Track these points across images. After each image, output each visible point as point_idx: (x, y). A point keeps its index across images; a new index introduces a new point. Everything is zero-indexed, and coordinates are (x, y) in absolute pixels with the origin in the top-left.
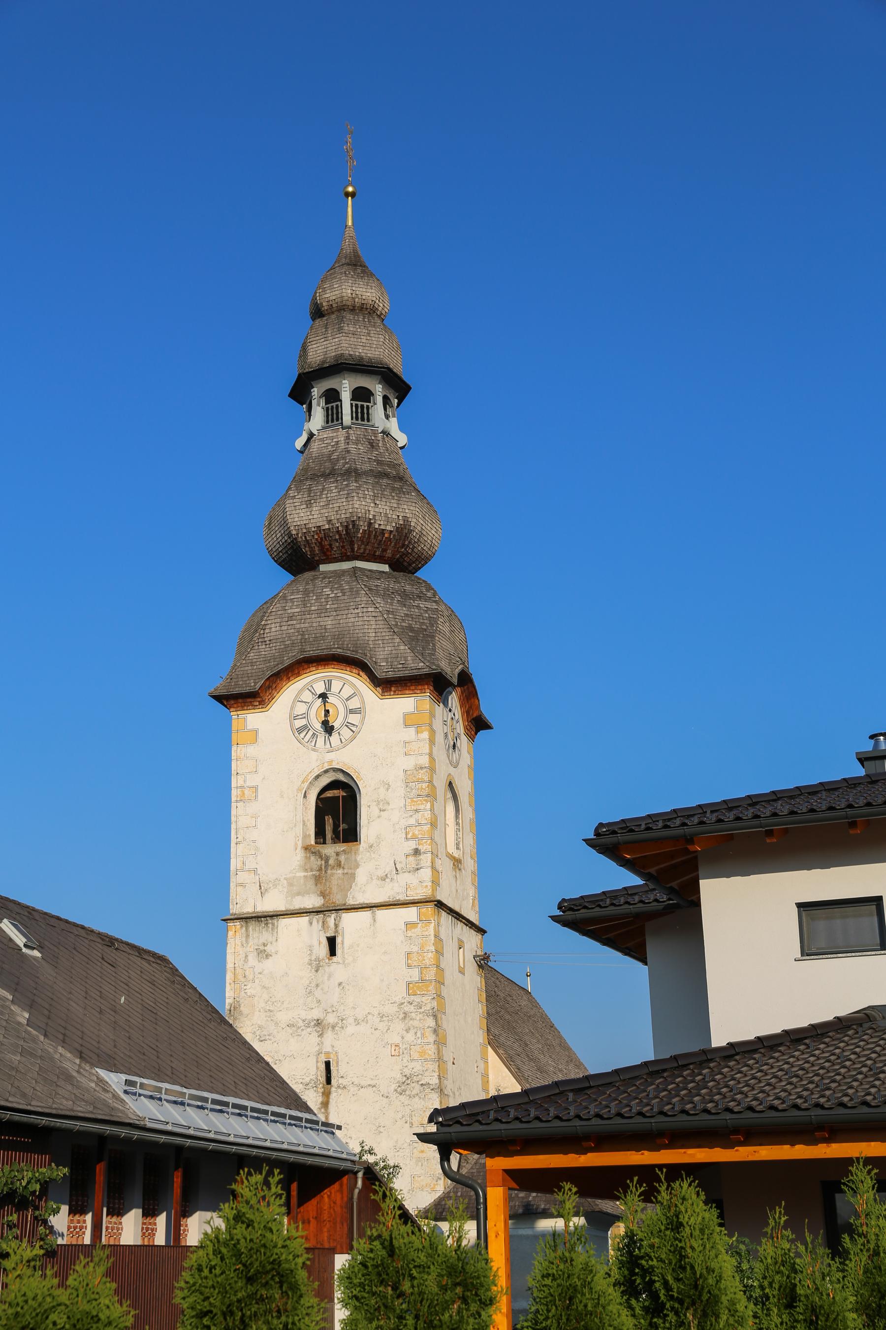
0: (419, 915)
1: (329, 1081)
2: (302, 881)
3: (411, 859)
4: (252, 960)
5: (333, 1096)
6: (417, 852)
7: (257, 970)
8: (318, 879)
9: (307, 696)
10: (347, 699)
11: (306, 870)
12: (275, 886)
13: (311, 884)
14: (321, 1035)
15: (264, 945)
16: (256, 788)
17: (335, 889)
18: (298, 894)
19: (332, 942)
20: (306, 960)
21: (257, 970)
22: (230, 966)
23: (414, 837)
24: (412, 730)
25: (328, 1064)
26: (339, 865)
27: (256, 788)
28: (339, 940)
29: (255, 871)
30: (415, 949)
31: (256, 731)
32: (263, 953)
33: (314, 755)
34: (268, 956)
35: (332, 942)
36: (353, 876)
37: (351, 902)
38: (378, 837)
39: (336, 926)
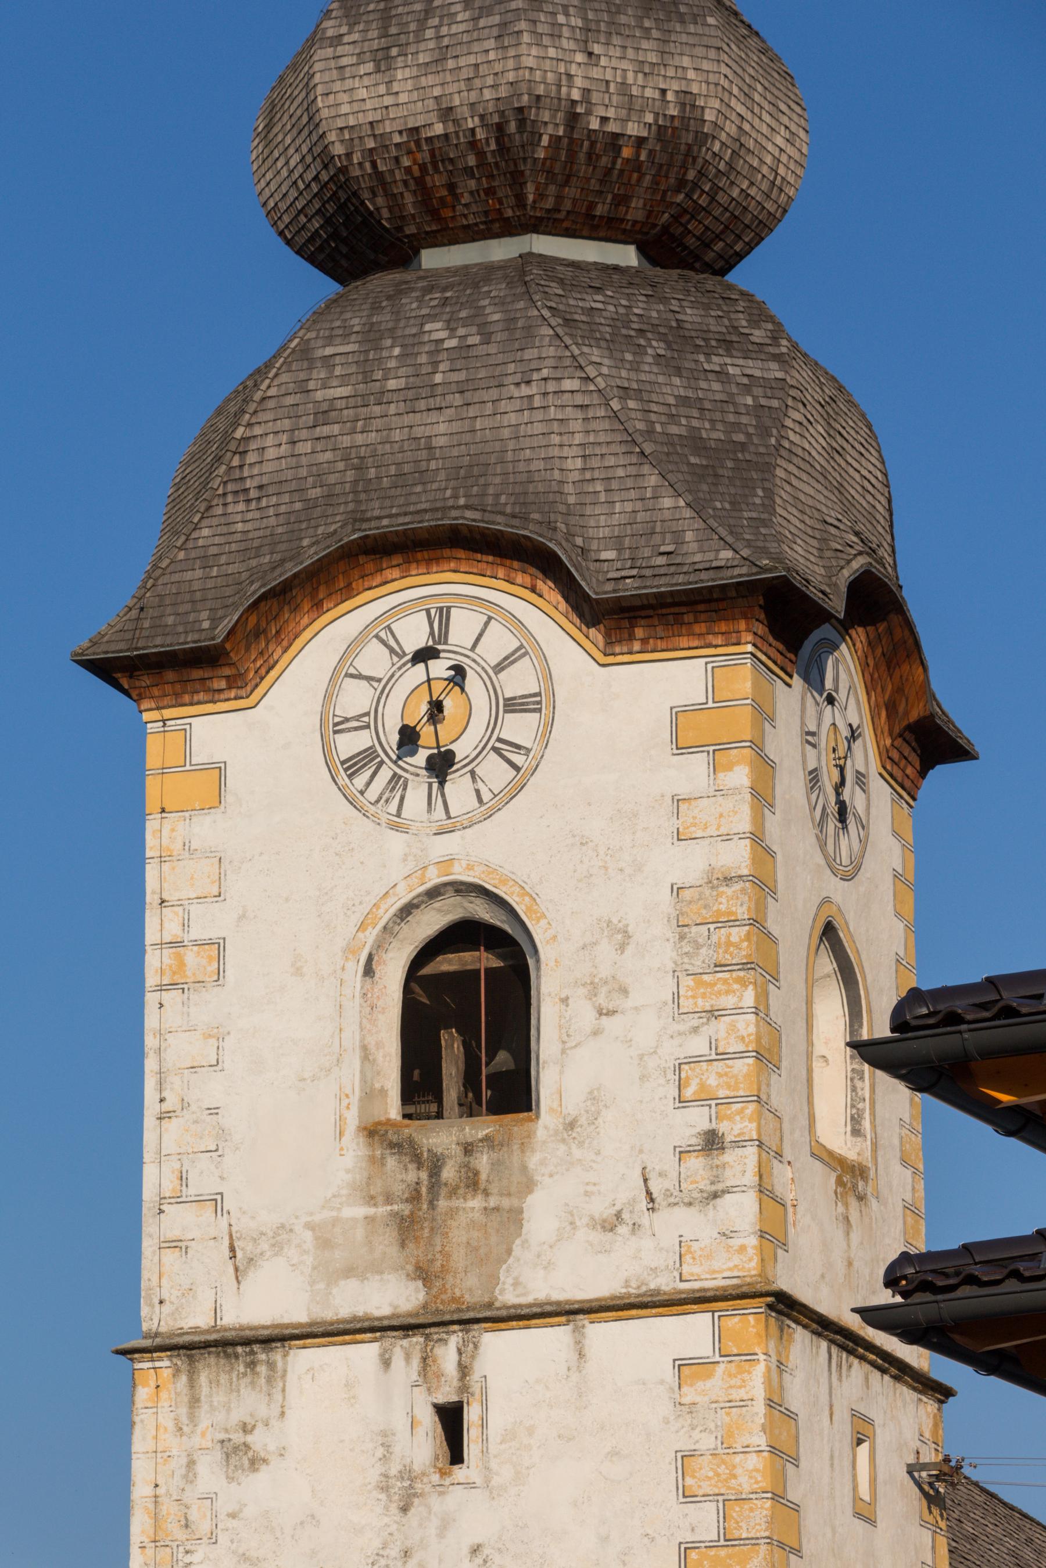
0: (719, 1336)
2: (360, 1233)
3: (696, 1163)
4: (210, 1475)
6: (712, 1142)
7: (224, 1506)
8: (406, 1228)
9: (374, 660)
10: (499, 668)
11: (371, 1200)
12: (278, 1248)
13: (386, 1242)
15: (246, 1429)
16: (219, 946)
17: (459, 1258)
18: (349, 1272)
19: (451, 1419)
20: (374, 1475)
21: (224, 1506)
22: (141, 1491)
23: (704, 1098)
24: (699, 763)
26: (472, 1182)
27: (219, 946)
29: (216, 1202)
30: (707, 1442)
31: (220, 770)
32: (240, 1455)
33: (396, 842)
34: (256, 1463)
35: (451, 1419)
36: (514, 1218)
37: (509, 1296)
38: (593, 1097)
39: (464, 1370)
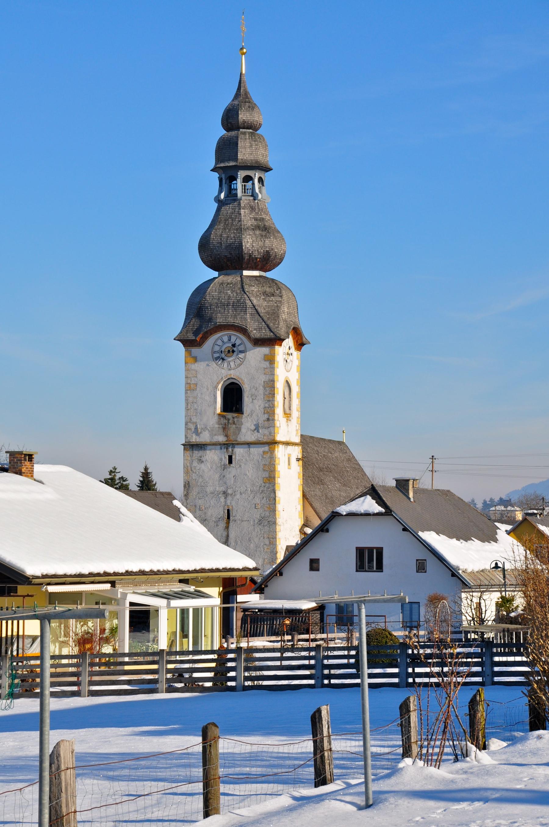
1: (229, 517)
2: (217, 429)
3: (266, 422)
4: (195, 464)
5: (231, 524)
8: (224, 429)
13: (221, 430)
14: (225, 498)
15: (201, 457)
19: (230, 458)
25: (228, 511)
26: (234, 423)
28: (233, 457)
32: (201, 461)
35: (230, 458)
